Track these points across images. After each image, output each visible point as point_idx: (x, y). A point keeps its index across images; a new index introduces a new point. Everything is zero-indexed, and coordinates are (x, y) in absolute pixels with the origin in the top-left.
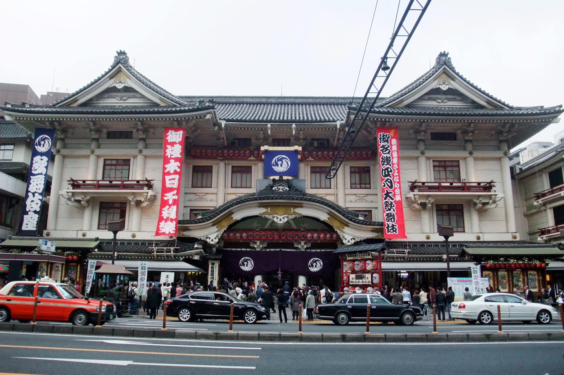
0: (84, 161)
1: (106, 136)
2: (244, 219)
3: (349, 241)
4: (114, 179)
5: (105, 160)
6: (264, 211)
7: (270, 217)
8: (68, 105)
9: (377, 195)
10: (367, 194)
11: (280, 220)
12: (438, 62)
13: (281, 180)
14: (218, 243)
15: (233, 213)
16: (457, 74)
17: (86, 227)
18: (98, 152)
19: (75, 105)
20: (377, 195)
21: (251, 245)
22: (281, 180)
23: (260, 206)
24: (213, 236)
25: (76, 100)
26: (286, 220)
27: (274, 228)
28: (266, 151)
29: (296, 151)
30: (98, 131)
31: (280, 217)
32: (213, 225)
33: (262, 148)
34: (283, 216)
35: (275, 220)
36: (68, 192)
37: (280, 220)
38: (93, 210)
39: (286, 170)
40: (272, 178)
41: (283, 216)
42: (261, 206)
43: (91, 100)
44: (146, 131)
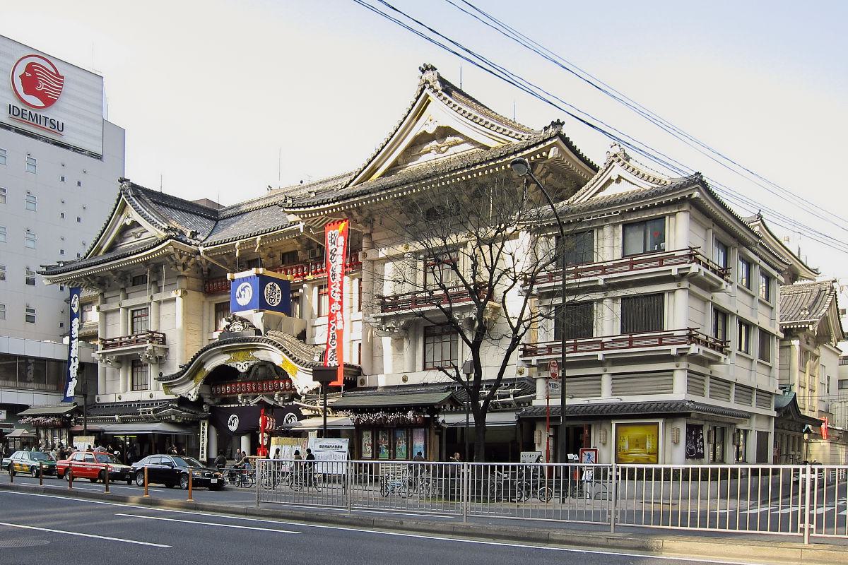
0: (116, 315)
1: (131, 283)
4: (139, 333)
5: (133, 312)
6: (227, 359)
7: (233, 365)
8: (96, 254)
15: (204, 364)
17: (121, 389)
18: (126, 303)
19: (101, 254)
23: (225, 353)
24: (192, 392)
25: (100, 248)
31: (242, 365)
32: (191, 379)
34: (244, 363)
35: (239, 368)
36: (376, 318)
38: (127, 367)
41: (244, 363)
42: (225, 351)
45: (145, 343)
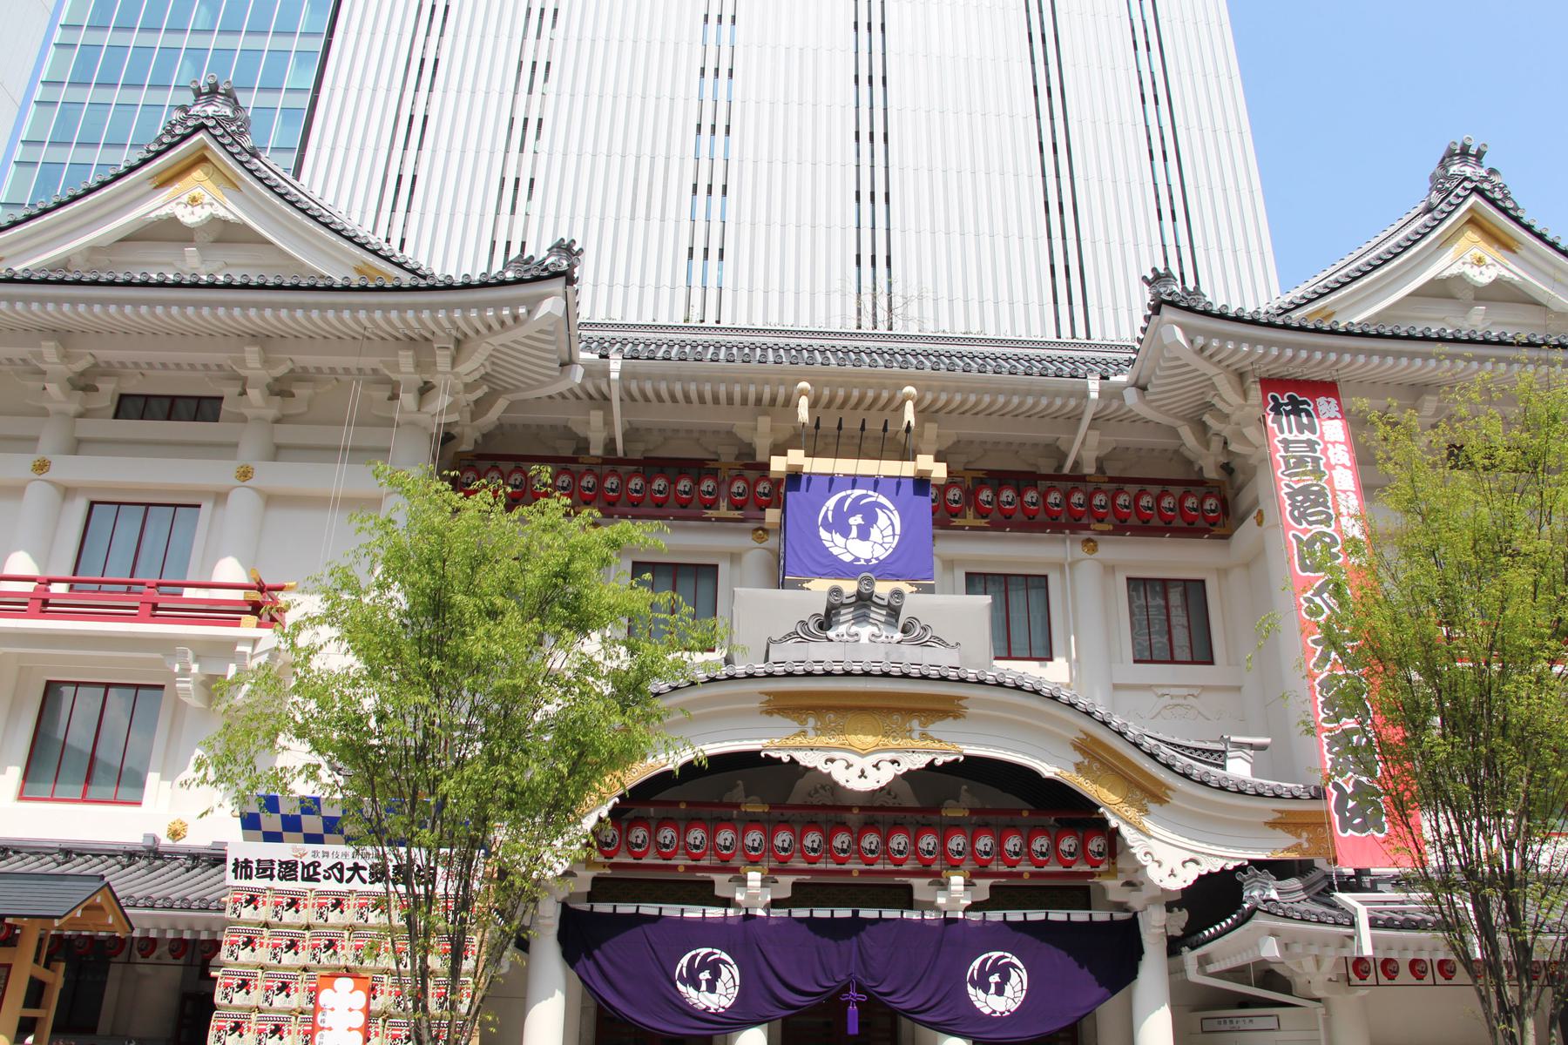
2: (690, 770)
3: (1172, 874)
7: (806, 759)
9: (1239, 689)
10: (1204, 688)
11: (862, 774)
12: (1442, 183)
13: (864, 601)
14: (567, 874)
16: (1528, 228)
20: (1239, 689)
21: (719, 892)
22: (864, 601)
26: (887, 775)
27: (827, 807)
28: (794, 478)
29: (921, 483)
30: (83, 384)
33: (778, 465)
37: (862, 774)
39: (882, 553)
40: (820, 587)
43: (65, 263)
44: (280, 389)
45: (236, 623)
